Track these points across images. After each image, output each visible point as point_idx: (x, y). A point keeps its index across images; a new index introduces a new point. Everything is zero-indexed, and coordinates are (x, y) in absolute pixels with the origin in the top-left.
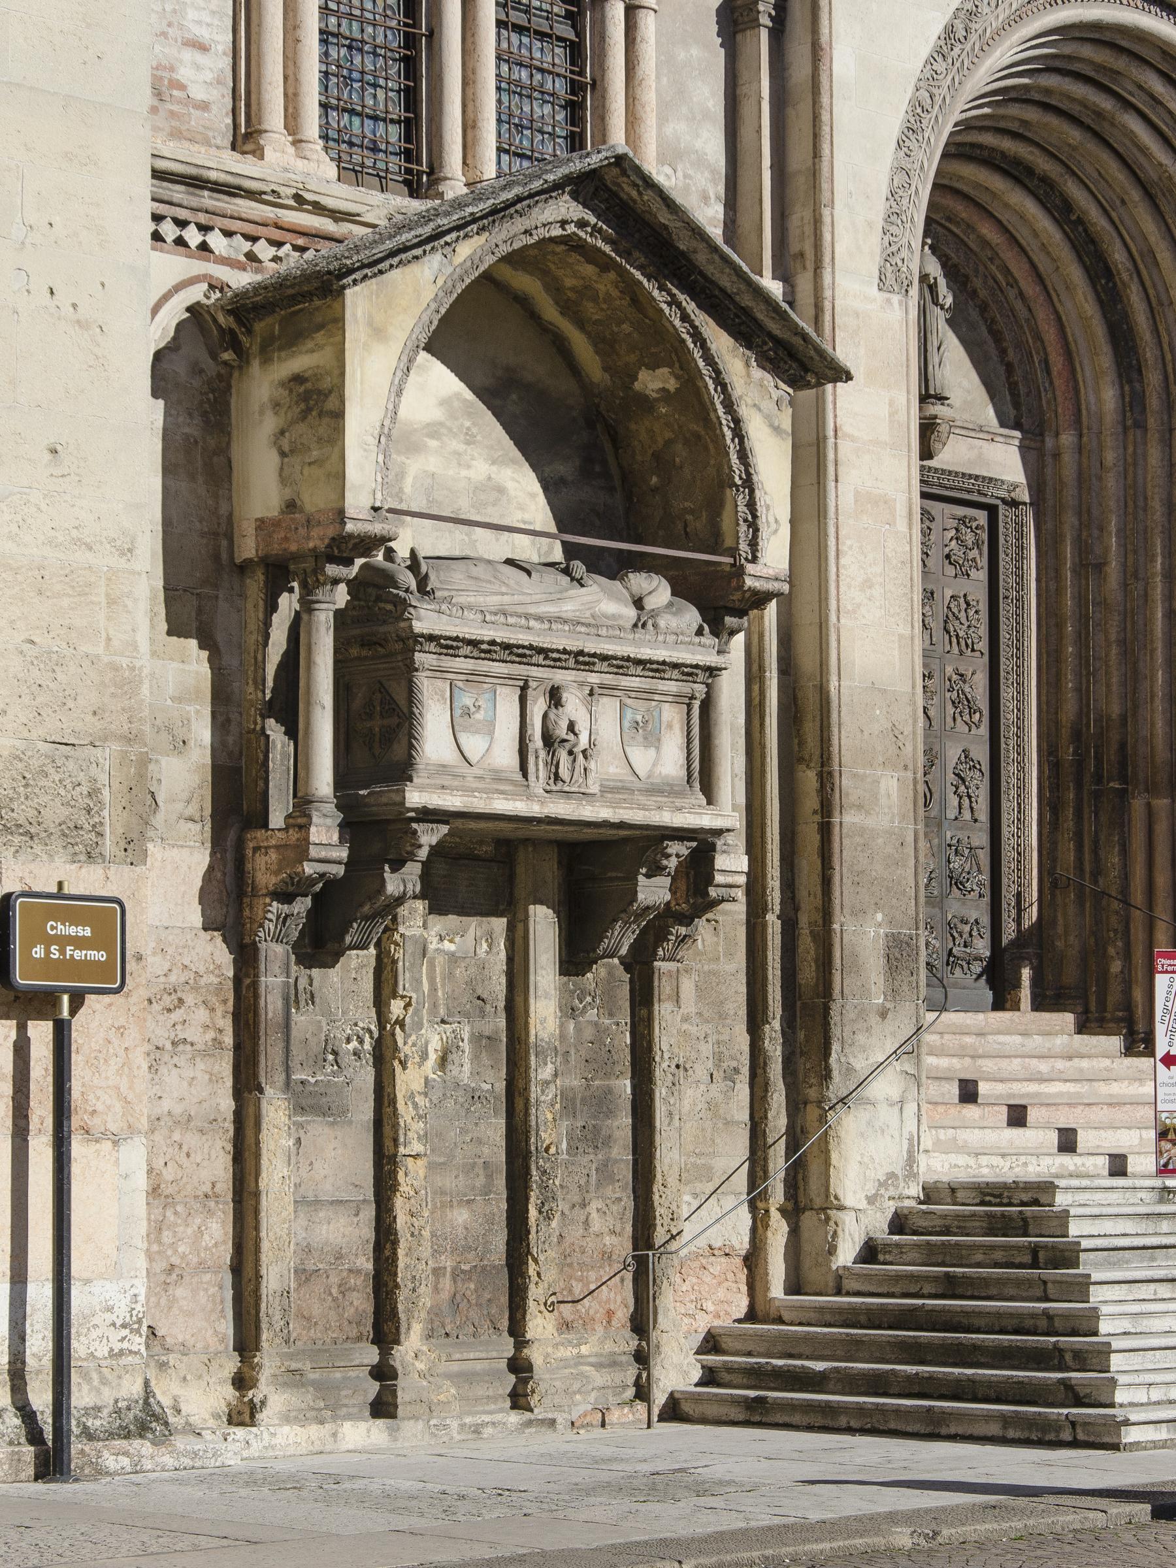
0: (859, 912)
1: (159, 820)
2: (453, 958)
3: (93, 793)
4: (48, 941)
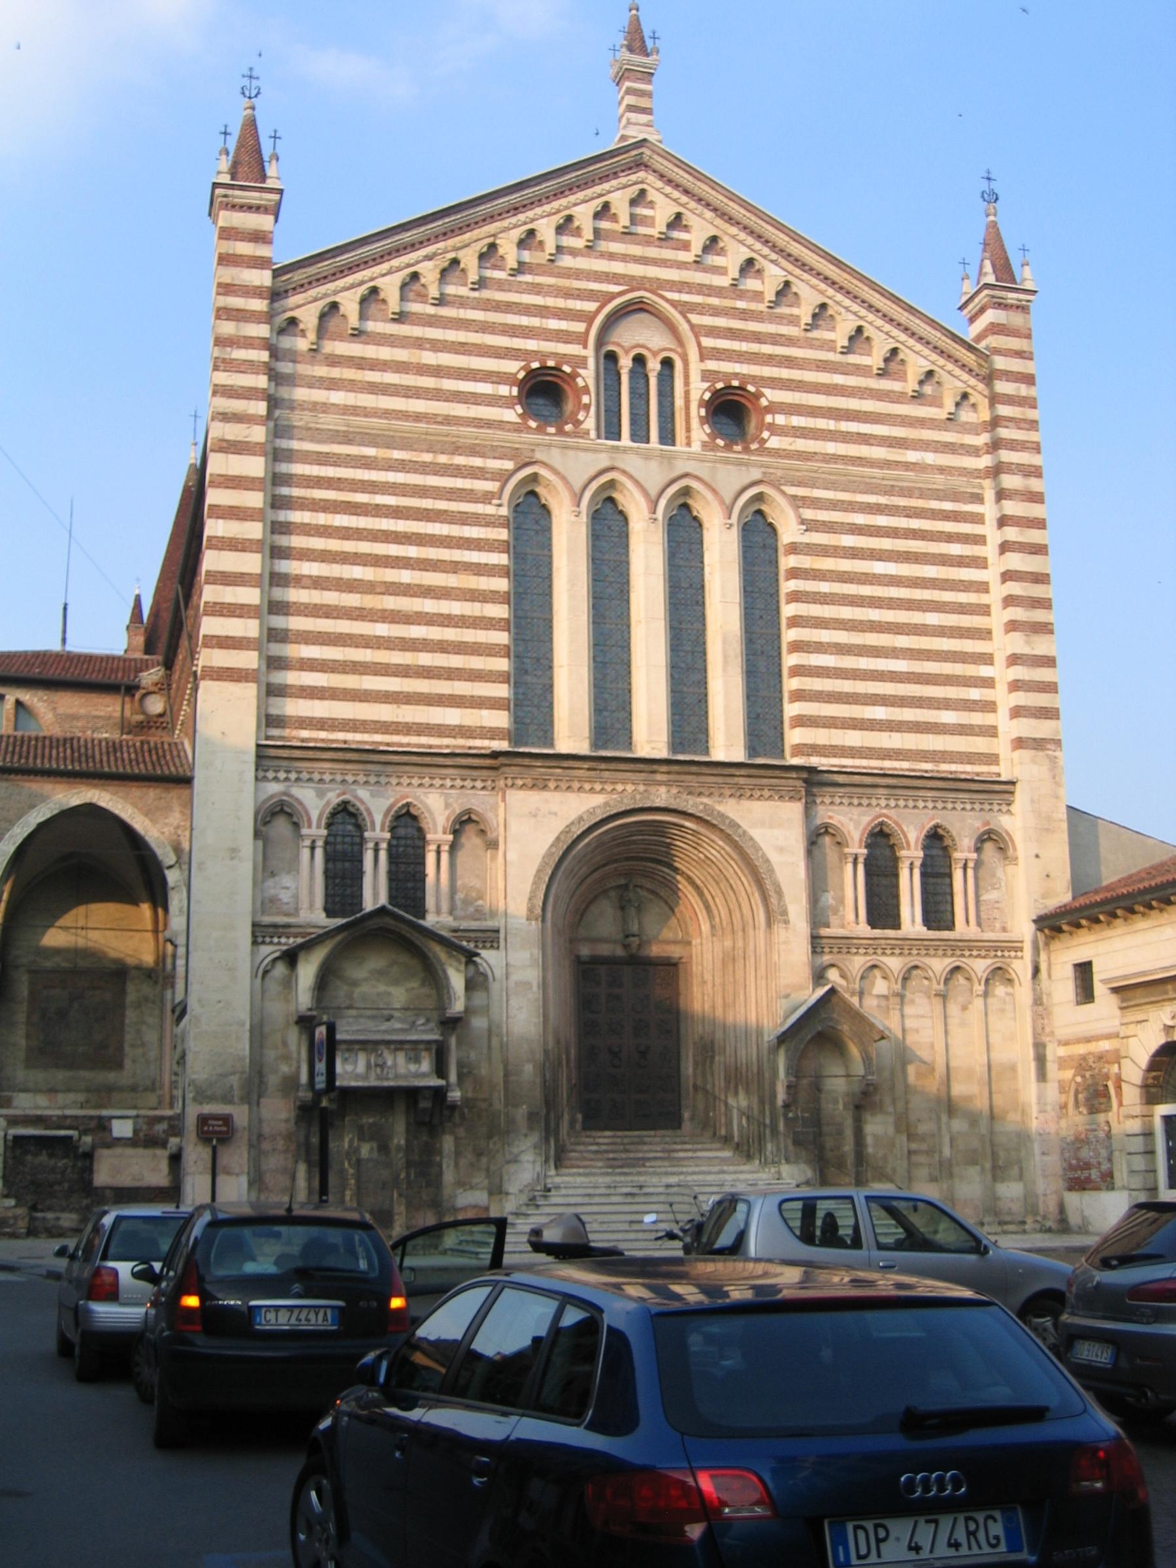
0: (516, 1106)
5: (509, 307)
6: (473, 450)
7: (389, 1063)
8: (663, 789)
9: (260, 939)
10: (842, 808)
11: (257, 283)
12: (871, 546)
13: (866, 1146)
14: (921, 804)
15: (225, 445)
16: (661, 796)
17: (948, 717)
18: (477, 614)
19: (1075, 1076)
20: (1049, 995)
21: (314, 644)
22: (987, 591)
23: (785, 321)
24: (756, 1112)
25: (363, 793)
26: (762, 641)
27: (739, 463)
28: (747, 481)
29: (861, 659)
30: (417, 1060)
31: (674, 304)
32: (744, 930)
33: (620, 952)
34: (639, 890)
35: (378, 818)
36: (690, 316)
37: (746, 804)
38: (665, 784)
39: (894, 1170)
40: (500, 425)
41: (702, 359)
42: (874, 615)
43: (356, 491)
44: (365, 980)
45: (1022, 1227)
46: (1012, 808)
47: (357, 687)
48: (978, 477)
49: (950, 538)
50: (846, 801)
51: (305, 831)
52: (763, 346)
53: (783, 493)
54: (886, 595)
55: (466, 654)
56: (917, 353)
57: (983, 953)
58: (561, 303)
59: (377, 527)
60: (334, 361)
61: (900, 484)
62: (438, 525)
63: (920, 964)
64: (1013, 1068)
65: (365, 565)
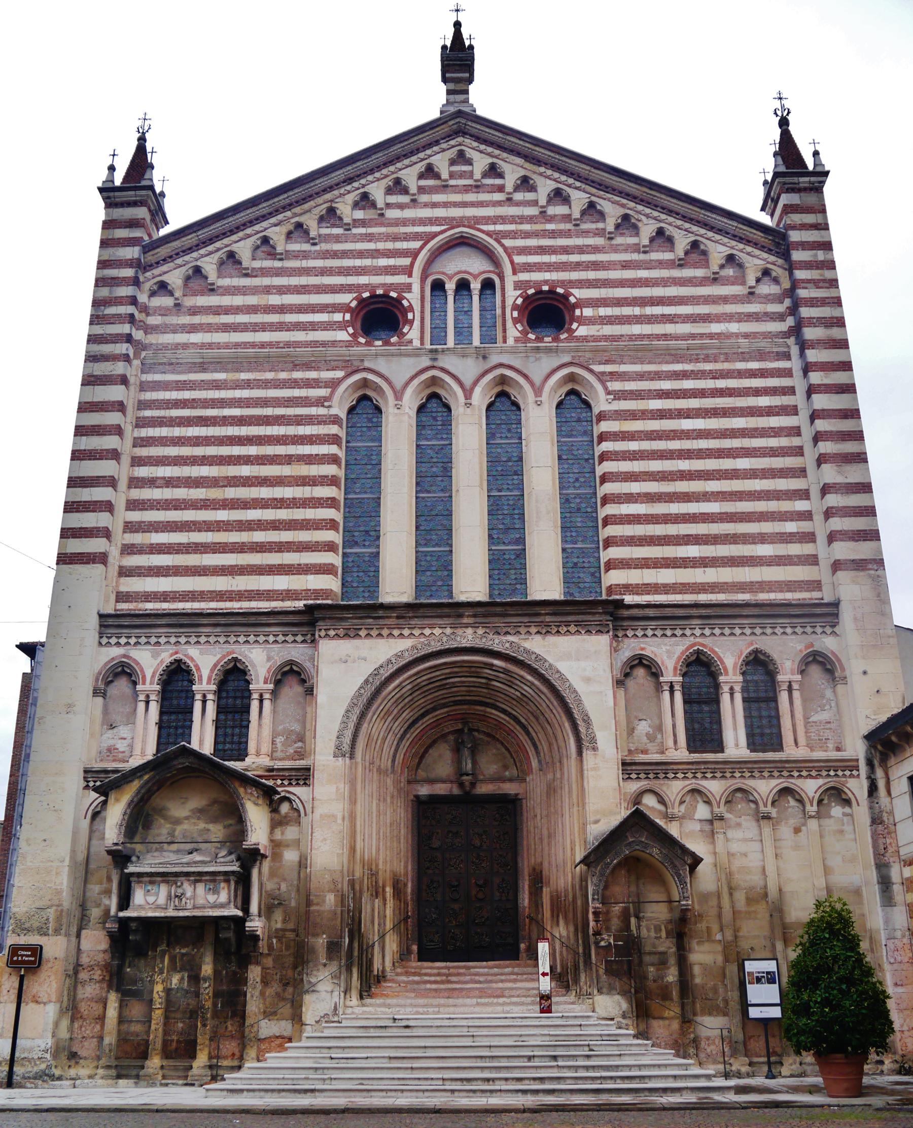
2: (183, 955)
3: (47, 919)
4: (18, 956)
5: (345, 254)
6: (308, 366)
7: (189, 894)
8: (470, 631)
9: (91, 784)
10: (655, 639)
12: (678, 407)
13: (693, 976)
14: (738, 631)
15: (92, 379)
16: (468, 637)
20: (891, 813)
21: (162, 531)
22: (799, 434)
23: (591, 235)
24: (572, 941)
26: (578, 500)
27: (549, 350)
28: (556, 362)
29: (671, 505)
30: (216, 891)
31: (488, 234)
32: (560, 762)
33: (456, 791)
34: (476, 734)
35: (205, 673)
36: (504, 241)
37: (552, 639)
38: (474, 626)
39: (726, 1002)
40: (334, 343)
41: (515, 272)
42: (684, 465)
44: (187, 818)
45: (880, 1067)
46: (836, 629)
47: (198, 564)
49: (757, 392)
50: (659, 633)
51: (139, 687)
52: (571, 256)
53: (591, 371)
54: (695, 447)
55: (295, 530)
57: (814, 773)
58: (390, 245)
59: (223, 434)
60: (194, 311)
61: (705, 352)
62: (276, 428)
63: (744, 787)
64: (857, 892)
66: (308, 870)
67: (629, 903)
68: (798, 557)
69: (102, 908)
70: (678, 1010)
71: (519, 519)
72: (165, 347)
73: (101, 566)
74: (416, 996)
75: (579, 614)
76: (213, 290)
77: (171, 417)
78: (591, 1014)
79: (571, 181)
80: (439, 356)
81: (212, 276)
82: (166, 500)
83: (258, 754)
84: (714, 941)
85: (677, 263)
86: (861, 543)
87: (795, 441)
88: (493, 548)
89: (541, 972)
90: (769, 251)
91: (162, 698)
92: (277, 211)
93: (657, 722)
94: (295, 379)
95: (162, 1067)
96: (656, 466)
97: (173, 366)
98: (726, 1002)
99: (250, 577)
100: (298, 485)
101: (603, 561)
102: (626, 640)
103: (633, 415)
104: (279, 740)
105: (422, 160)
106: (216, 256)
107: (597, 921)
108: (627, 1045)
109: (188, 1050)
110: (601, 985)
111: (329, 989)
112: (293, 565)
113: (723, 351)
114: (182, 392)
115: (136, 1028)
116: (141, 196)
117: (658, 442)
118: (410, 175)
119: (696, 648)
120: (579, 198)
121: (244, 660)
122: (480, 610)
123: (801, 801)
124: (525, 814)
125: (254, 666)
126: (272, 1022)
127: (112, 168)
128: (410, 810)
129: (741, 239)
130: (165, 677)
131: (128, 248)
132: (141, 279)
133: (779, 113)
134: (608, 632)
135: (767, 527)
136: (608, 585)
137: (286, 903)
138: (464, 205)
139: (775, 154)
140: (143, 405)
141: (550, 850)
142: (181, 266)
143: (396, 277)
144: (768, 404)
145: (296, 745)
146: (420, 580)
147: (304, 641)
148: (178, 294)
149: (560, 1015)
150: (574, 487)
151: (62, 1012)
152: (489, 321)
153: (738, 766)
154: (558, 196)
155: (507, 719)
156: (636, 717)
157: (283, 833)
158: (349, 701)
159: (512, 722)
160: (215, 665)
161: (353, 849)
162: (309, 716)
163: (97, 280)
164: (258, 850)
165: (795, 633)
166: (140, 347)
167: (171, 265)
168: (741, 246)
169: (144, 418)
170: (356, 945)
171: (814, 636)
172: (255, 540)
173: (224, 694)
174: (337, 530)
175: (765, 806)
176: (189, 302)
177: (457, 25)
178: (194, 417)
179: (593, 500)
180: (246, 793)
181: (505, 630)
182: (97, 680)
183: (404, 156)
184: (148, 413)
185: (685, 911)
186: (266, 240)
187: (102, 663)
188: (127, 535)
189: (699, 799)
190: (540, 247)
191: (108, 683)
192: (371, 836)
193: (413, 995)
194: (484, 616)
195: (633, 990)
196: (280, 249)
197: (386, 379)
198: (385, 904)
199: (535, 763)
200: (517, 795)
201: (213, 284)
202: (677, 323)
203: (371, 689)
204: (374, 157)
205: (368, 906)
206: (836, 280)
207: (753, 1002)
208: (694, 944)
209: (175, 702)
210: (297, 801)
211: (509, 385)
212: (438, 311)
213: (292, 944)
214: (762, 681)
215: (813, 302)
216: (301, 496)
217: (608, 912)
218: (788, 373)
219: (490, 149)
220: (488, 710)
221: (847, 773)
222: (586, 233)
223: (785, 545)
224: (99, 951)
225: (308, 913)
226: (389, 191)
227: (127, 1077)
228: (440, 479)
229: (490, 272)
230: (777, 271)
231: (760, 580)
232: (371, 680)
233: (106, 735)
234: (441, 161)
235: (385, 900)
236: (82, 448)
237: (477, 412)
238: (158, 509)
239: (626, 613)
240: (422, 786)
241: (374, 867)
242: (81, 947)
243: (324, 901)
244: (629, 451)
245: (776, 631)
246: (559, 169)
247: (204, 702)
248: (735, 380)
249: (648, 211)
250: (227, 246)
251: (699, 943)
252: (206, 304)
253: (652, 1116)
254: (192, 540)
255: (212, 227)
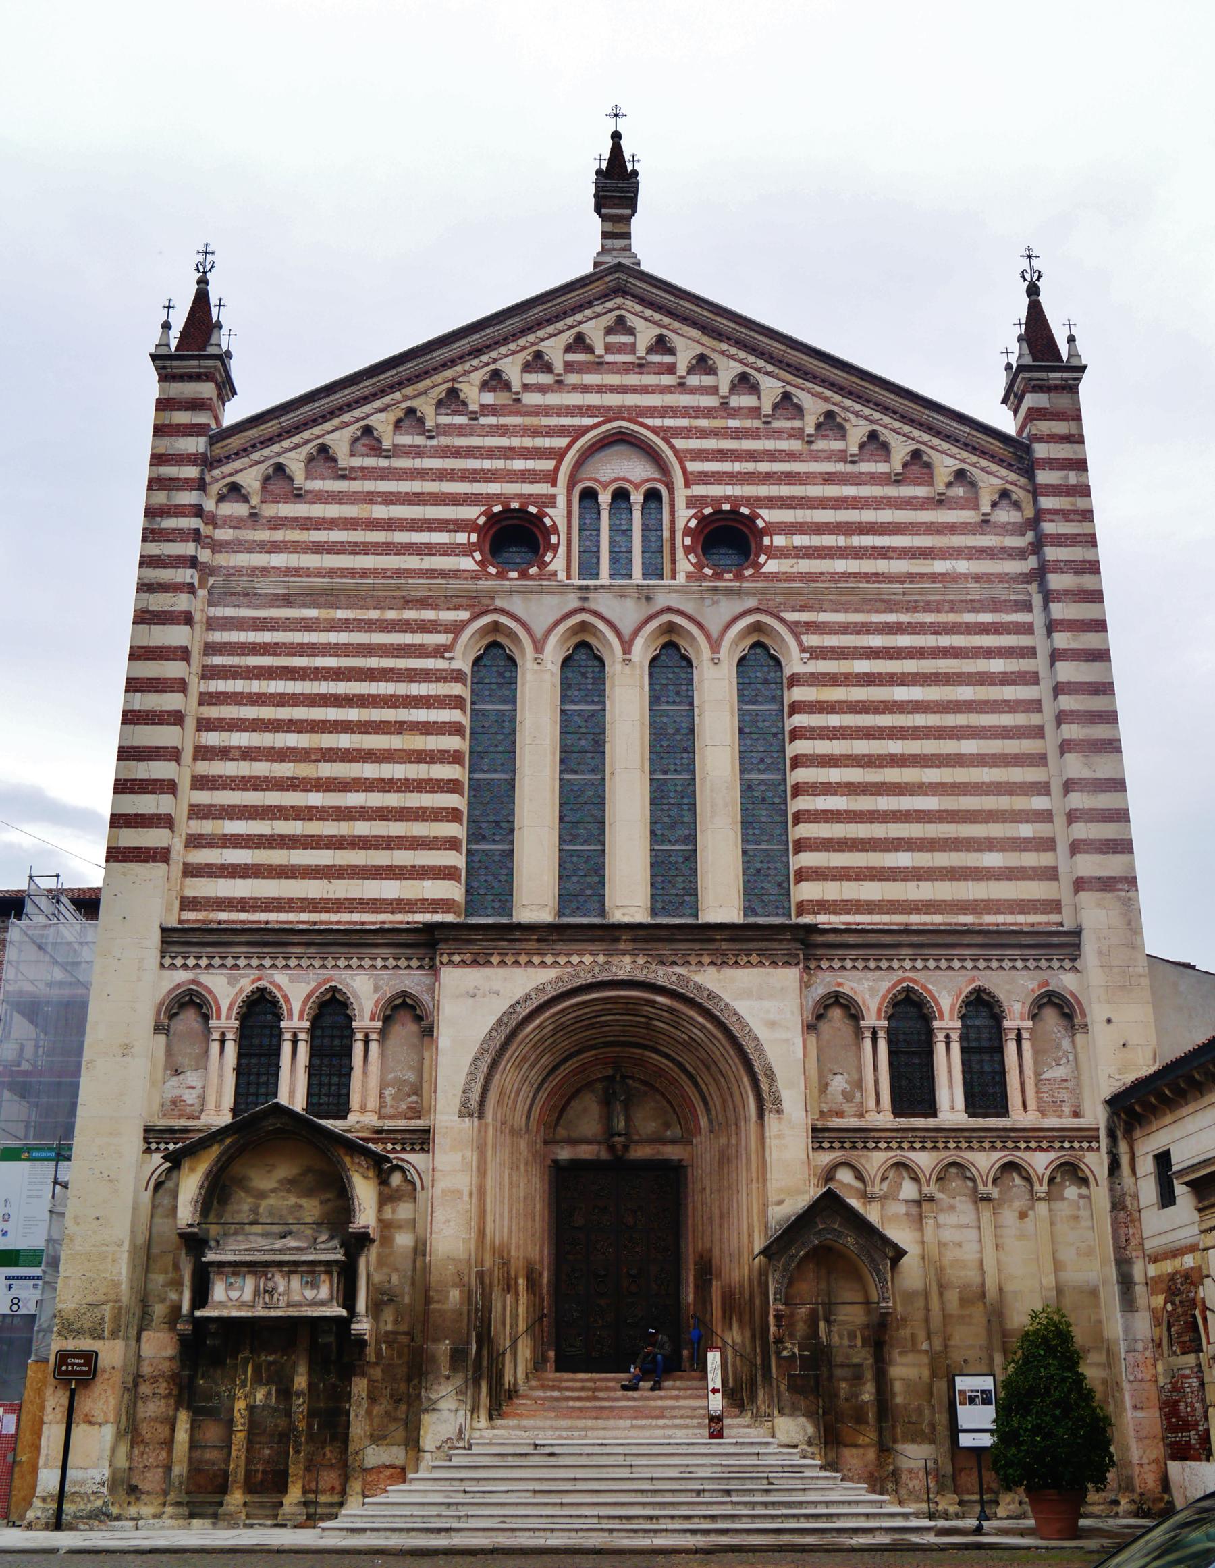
1: (154, 1324)
2: (270, 1363)
3: (102, 1318)
4: (68, 1365)
5: (469, 452)
6: (423, 604)
7: (281, 1289)
8: (627, 959)
9: (153, 1146)
10: (856, 973)
11: (192, 450)
13: (894, 1395)
14: (956, 964)
15: (147, 616)
16: (625, 967)
17: (992, 859)
18: (424, 776)
19: (1166, 1303)
20: (1135, 1196)
21: (238, 819)
23: (785, 436)
24: (748, 1350)
25: (281, 978)
26: (763, 788)
27: (729, 591)
28: (739, 608)
29: (879, 798)
30: (315, 1285)
31: (654, 430)
32: (736, 1125)
33: (604, 1155)
34: (630, 1082)
35: (296, 1006)
36: (674, 441)
37: (728, 972)
38: (633, 953)
39: (933, 1426)
40: (456, 573)
41: (687, 485)
42: (895, 747)
43: (294, 655)
44: (274, 1191)
45: (1115, 1508)
47: (284, 862)
48: (1022, 583)
49: (989, 653)
50: (860, 964)
51: (212, 1023)
52: (759, 464)
53: (782, 620)
54: (910, 724)
55: (408, 820)
56: (943, 452)
57: (1044, 1145)
58: (528, 442)
60: (276, 523)
63: (960, 1160)
64: (1093, 1293)
65: (300, 732)
66: (428, 1259)
67: (817, 1304)
68: (1034, 869)
69: (168, 1303)
70: (874, 1436)
71: (689, 810)
72: (238, 572)
73: (163, 866)
74: (557, 1417)
75: (762, 940)
76: (299, 496)
77: (248, 667)
78: (770, 1440)
79: (761, 363)
80: (591, 596)
81: (300, 479)
82: (243, 777)
83: (363, 1110)
84: (920, 1352)
85: (894, 478)
86: (1110, 856)
87: (1035, 719)
88: (656, 848)
89: (710, 1388)
90: (1009, 467)
91: (241, 1037)
92: (382, 391)
93: (856, 1077)
94: (407, 620)
95: (245, 1504)
96: (860, 747)
97: (249, 598)
98: (933, 1426)
99: (351, 881)
100: (411, 762)
101: (793, 867)
102: (819, 973)
103: (834, 680)
104: (389, 1092)
105: (571, 327)
106: (304, 452)
107: (778, 1326)
108: (812, 1478)
109: (277, 1483)
110: (782, 1404)
111: (453, 1407)
112: (406, 867)
113: (948, 598)
114: (260, 634)
115: (211, 1455)
116: (206, 367)
117: (864, 716)
118: (554, 348)
119: (905, 985)
120: (771, 388)
121: (345, 990)
122: (640, 933)
123: (1028, 1179)
124: (690, 1186)
125: (357, 997)
126: (381, 1448)
127: (166, 326)
128: (546, 1177)
129: (974, 450)
130: (244, 1009)
131: (190, 438)
132: (208, 479)
133: (1028, 277)
134: (798, 964)
135: (996, 830)
136: (800, 899)
137: (399, 1299)
138: (623, 389)
139: (1020, 339)
140: (211, 649)
141: (721, 1233)
142: (258, 463)
143: (536, 485)
144: (1002, 669)
145: (410, 1099)
146: (565, 888)
147: (420, 967)
148: (255, 500)
149: (734, 1441)
150: (759, 770)
151: (119, 1436)
152: (653, 545)
153: (953, 1134)
154: (744, 382)
155: (671, 1065)
156: (830, 1070)
157: (394, 1212)
158: (478, 1046)
159: (676, 1069)
160: (309, 996)
161: (482, 1233)
162: (426, 1063)
163: (150, 481)
164: (367, 1234)
165: (1026, 967)
166: (206, 571)
167: (246, 460)
168: (974, 459)
169: (214, 666)
170: (485, 1353)
171: (1049, 972)
172: (357, 833)
173: (319, 1033)
174: (460, 821)
175: (985, 1185)
176: (270, 510)
177: (616, 136)
178: (278, 667)
179: (782, 788)
180: (353, 1163)
181: (671, 959)
182: (158, 1012)
183: (548, 321)
184: (217, 660)
185: (884, 1315)
186: (368, 430)
187: (164, 991)
188: (193, 823)
189: (905, 1175)
190: (720, 451)
191: (172, 1016)
192: (502, 1215)
193: (553, 1415)
194: (646, 940)
195: (821, 1411)
196: (386, 444)
197: (524, 625)
198: (517, 1300)
199: (704, 1122)
200: (681, 1161)
201: (300, 489)
202: (892, 558)
203: (505, 1031)
204: (508, 323)
205: (500, 1304)
206: (1091, 512)
207: (964, 1427)
208: (896, 1354)
209: (256, 1041)
210: (412, 1170)
211: (679, 634)
212: (589, 529)
213: (406, 1350)
214: (986, 1027)
215: (1061, 540)
216: (415, 776)
217: (792, 1315)
218: (1028, 629)
219: (657, 316)
220: (647, 1053)
221: (1085, 1145)
222: (778, 434)
223: (1017, 854)
224: (165, 1358)
225: (426, 1313)
226: (527, 368)
227: (201, 1516)
228: (590, 755)
229: (654, 480)
230: (1018, 494)
231: (986, 898)
232: (505, 1020)
233: (170, 1083)
234: (594, 330)
235: (517, 1294)
236: (137, 708)
237: (638, 671)
238: (233, 789)
239: (820, 939)
240: (562, 1148)
241: (505, 1255)
242: (142, 1354)
243: (447, 1298)
244: (827, 727)
245: (1004, 964)
246: (745, 346)
247: (295, 1042)
248: (962, 637)
249: (858, 407)
250: (318, 437)
251: (902, 1353)
252: (291, 515)
253: (839, 1558)
254: (277, 831)
255: (299, 412)
